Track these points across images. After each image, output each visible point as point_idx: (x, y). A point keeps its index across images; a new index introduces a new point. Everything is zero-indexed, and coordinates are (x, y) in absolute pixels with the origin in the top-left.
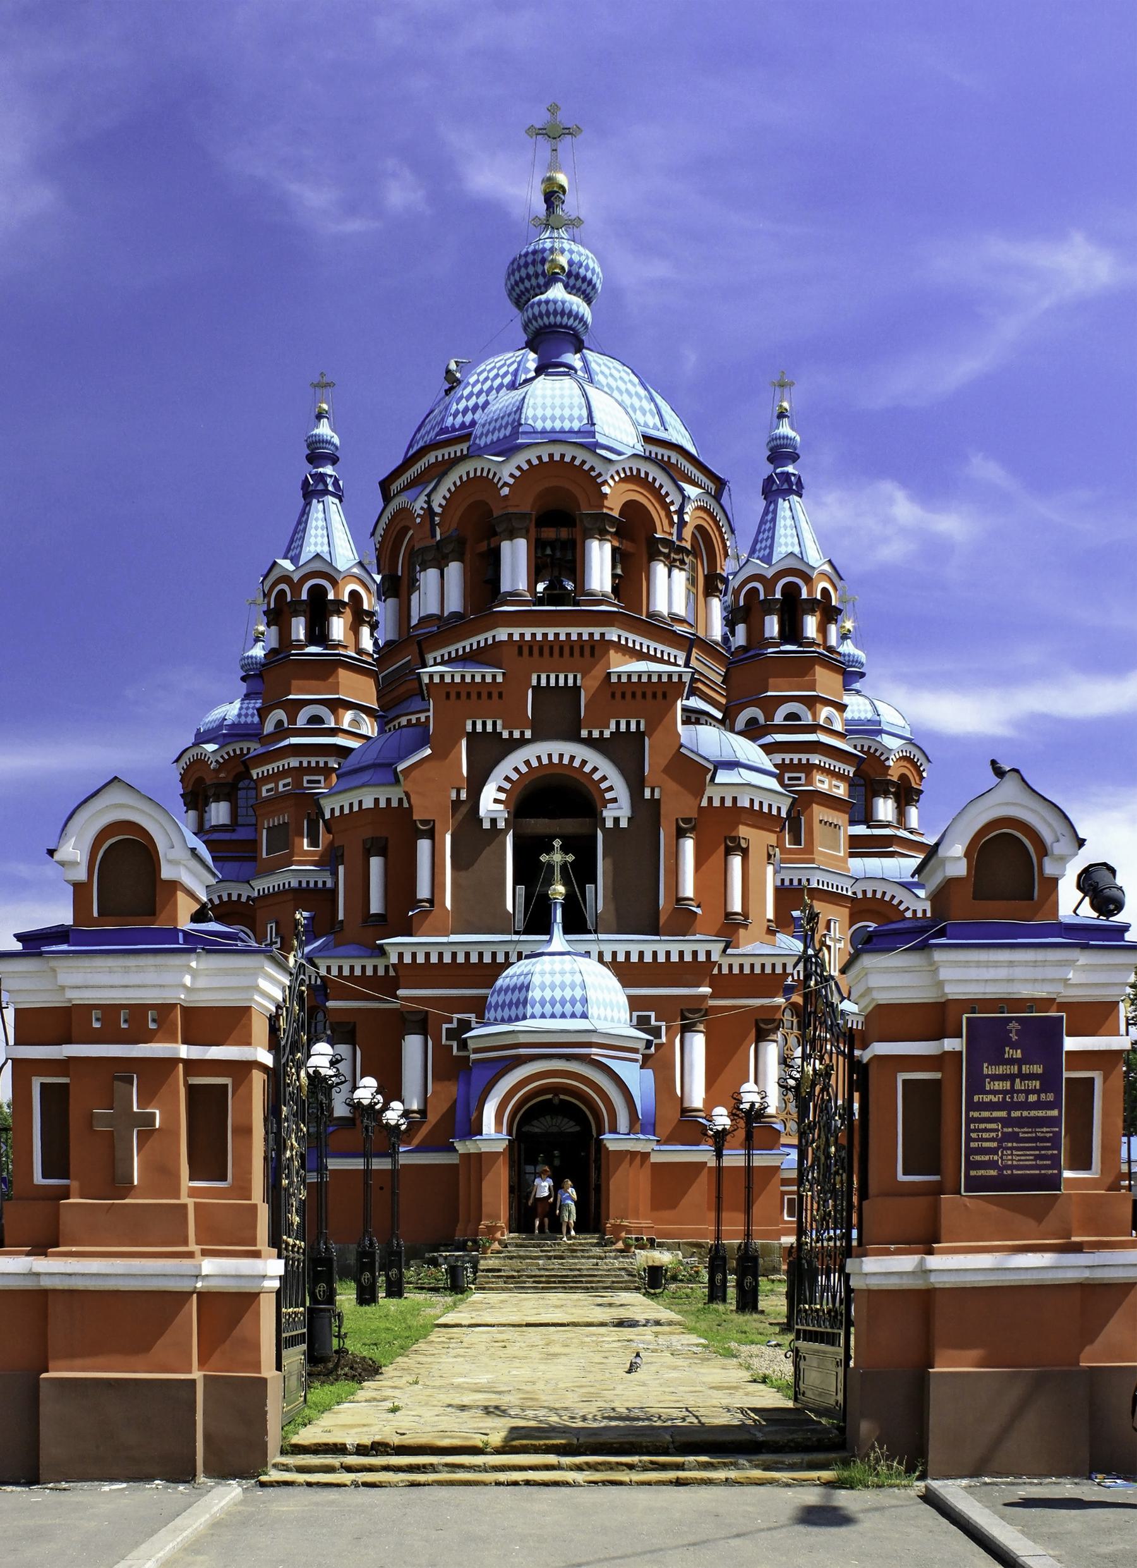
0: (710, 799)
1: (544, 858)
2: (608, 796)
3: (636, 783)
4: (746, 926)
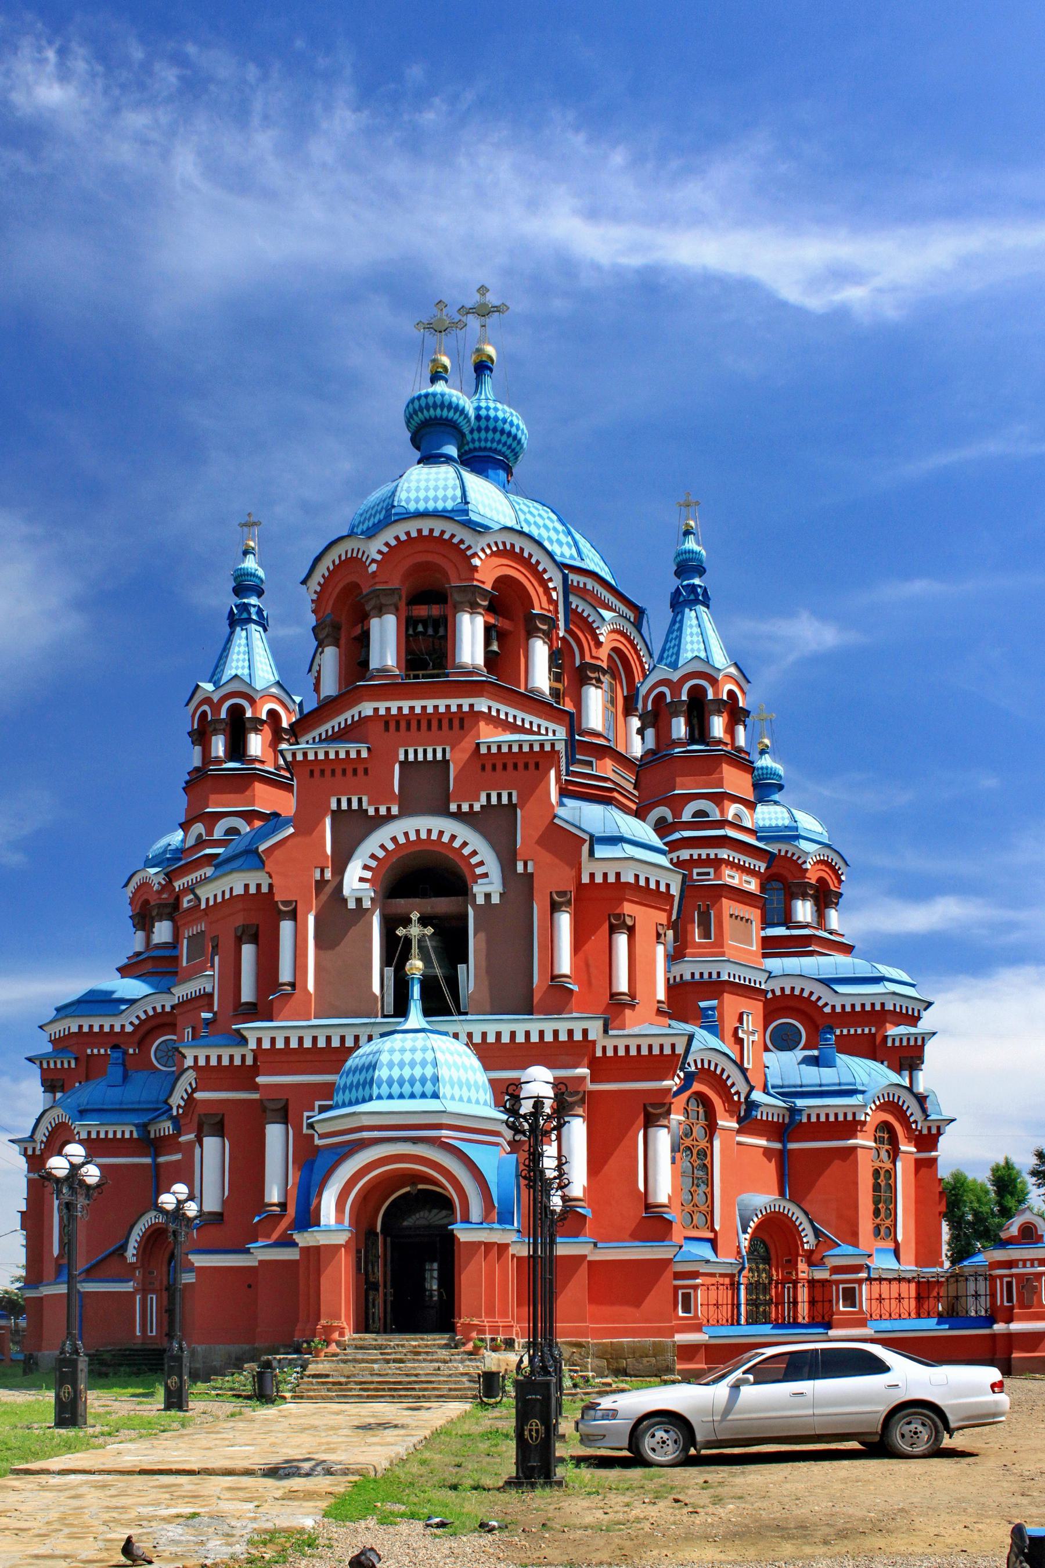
2: (479, 871)
3: (507, 858)
4: (633, 1007)
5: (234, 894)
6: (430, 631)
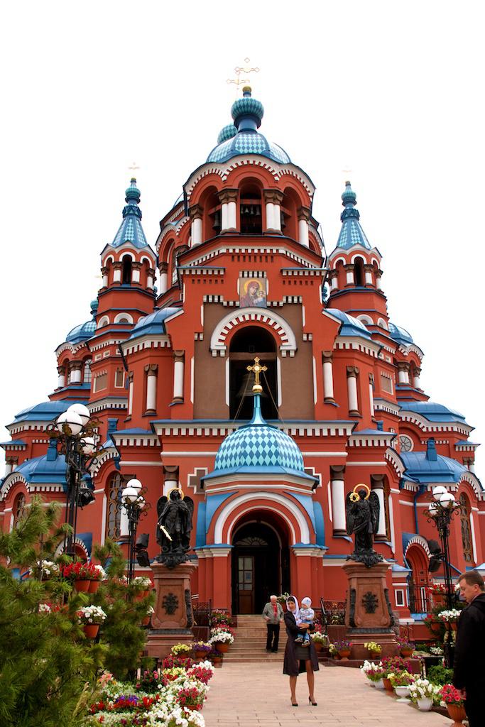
0: (338, 345)
1: (249, 368)
2: (283, 338)
3: (298, 333)
5: (145, 347)
6: (252, 213)
